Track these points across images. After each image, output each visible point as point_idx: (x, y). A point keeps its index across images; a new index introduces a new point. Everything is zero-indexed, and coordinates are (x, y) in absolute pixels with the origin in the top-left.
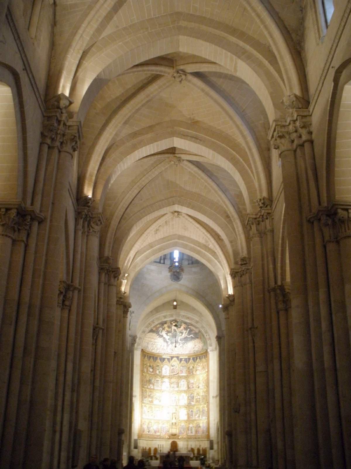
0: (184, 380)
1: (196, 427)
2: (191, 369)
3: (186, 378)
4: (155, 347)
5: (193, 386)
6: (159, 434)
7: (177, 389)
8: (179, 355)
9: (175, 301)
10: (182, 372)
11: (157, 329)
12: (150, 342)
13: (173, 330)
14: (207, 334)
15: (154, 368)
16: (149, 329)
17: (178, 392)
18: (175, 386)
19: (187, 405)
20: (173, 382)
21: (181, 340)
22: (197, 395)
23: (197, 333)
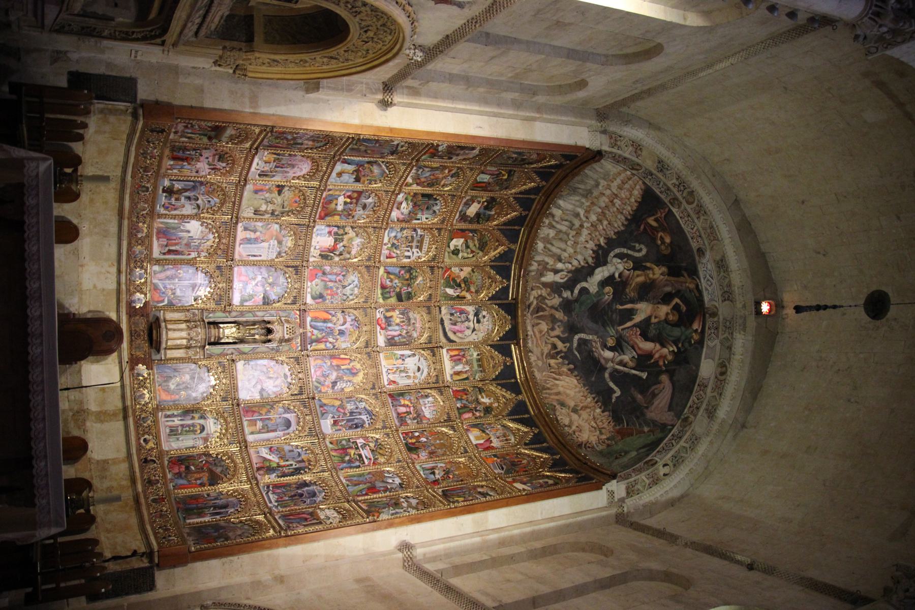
0: (426, 371)
1: (207, 455)
2: (477, 400)
3: (437, 382)
4: (560, 231)
5: (409, 421)
6: (156, 253)
7: (381, 341)
8: (524, 340)
9: (778, 306)
10: (456, 360)
11: (649, 237)
12: (588, 204)
13: (629, 306)
14: (671, 464)
15: (474, 226)
16: (675, 190)
17: (367, 347)
18: (394, 331)
19: (314, 398)
20: (409, 320)
21: (582, 342)
22: (372, 445)
23: (643, 414)
